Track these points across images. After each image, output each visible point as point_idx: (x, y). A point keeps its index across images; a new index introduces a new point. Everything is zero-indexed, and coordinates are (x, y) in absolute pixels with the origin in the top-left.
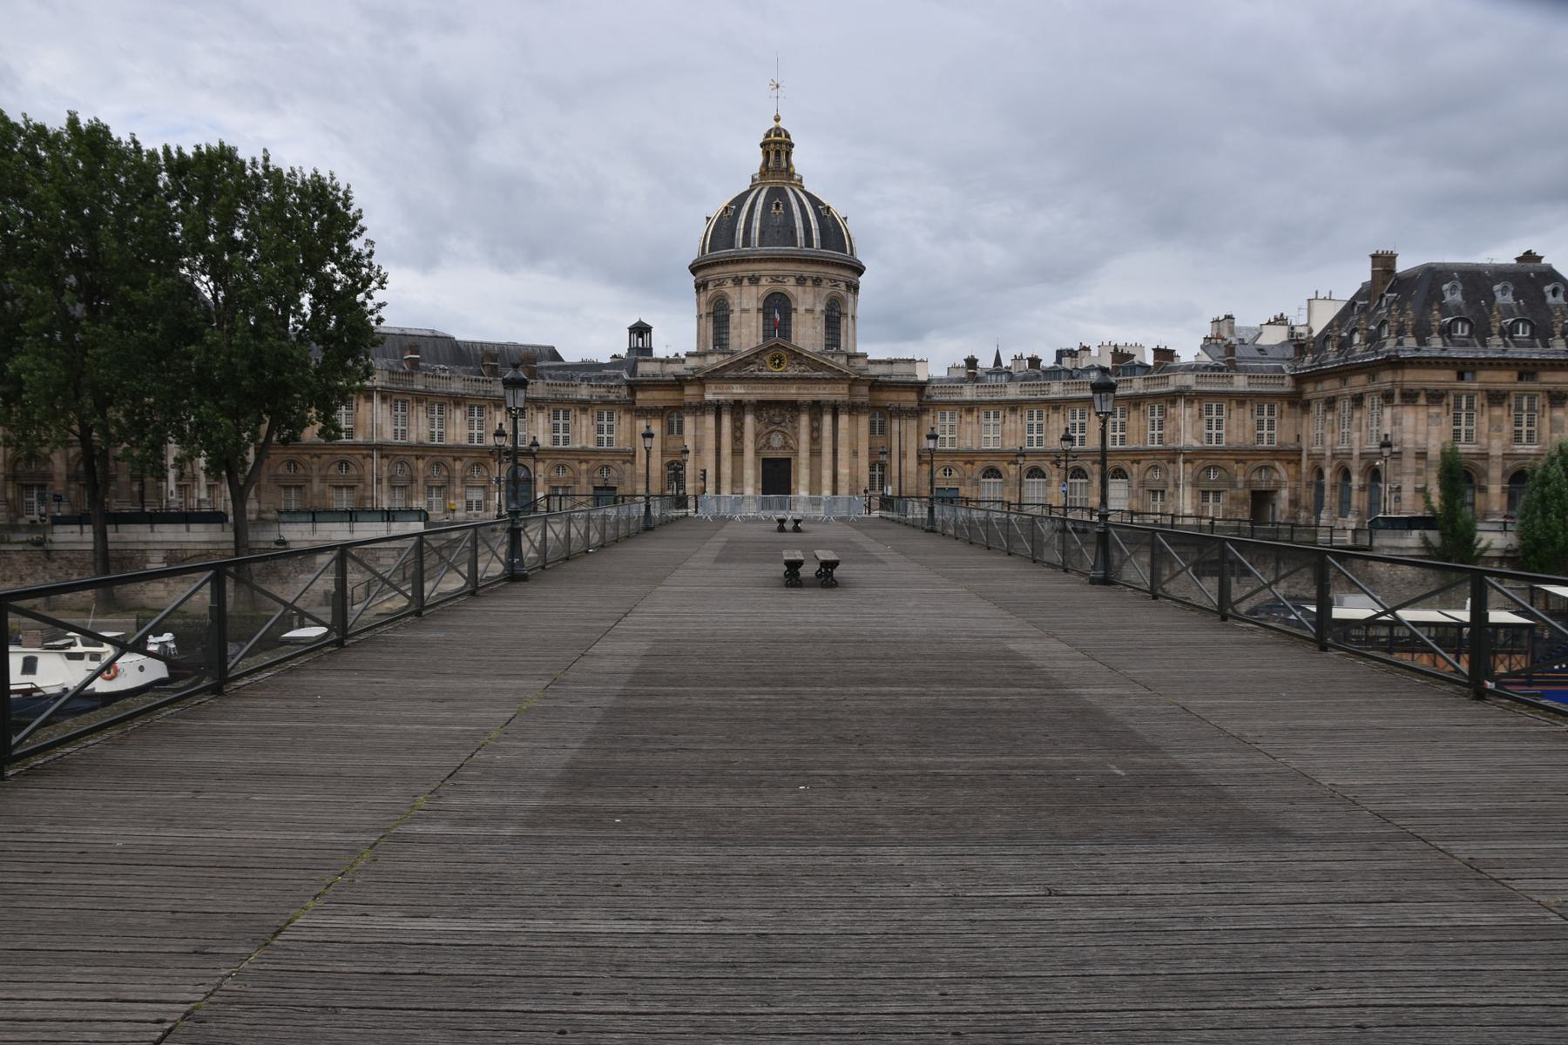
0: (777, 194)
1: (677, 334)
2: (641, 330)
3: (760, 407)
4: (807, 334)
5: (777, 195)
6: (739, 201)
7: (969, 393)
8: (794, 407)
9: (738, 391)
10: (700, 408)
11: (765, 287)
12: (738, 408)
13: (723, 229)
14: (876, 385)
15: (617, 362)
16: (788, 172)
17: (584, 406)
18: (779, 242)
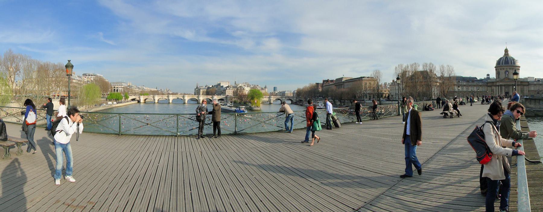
0: (506, 58)
1: (493, 75)
2: (488, 75)
3: (504, 85)
4: (511, 76)
5: (506, 58)
6: (501, 59)
7: (535, 83)
8: (509, 85)
9: (501, 83)
10: (496, 86)
11: (505, 70)
12: (501, 85)
13: (499, 62)
14: (521, 82)
15: (485, 79)
16: (508, 54)
17: (481, 86)
18: (506, 64)
